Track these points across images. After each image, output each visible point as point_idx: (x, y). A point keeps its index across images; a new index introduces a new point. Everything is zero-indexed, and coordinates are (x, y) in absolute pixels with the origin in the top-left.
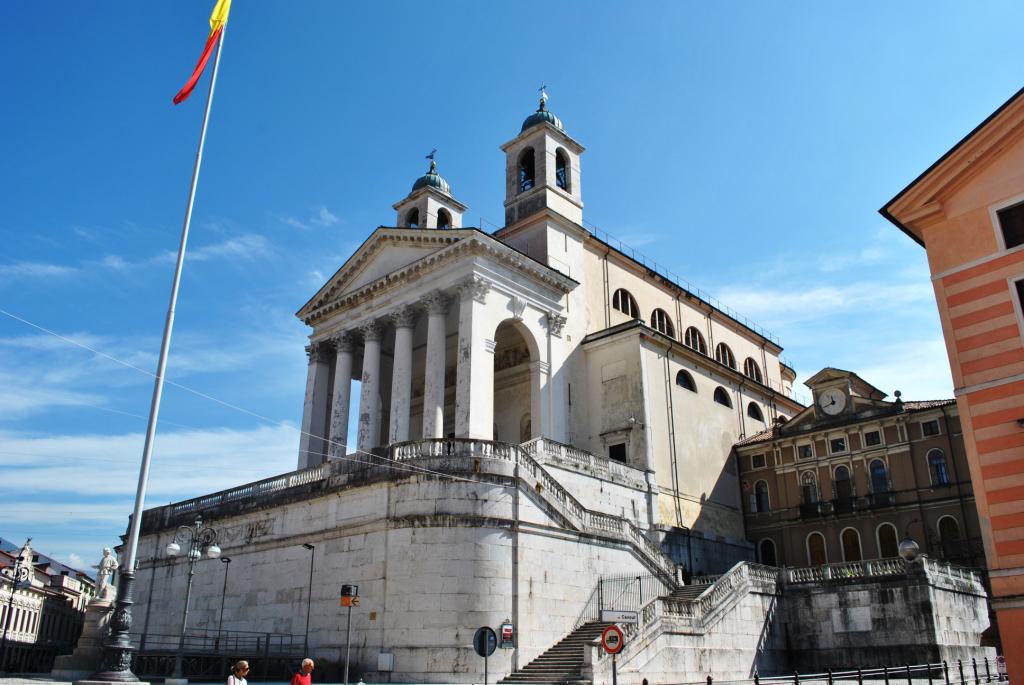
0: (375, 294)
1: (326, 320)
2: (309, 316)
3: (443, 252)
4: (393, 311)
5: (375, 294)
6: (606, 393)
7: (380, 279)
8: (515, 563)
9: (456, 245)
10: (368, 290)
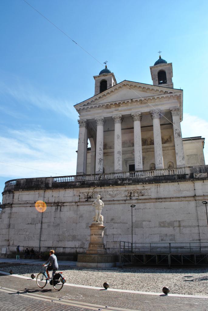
0: (121, 105)
1: (90, 111)
3: (160, 96)
4: (134, 113)
5: (121, 105)
6: (189, 159)
9: (171, 94)
10: (119, 103)
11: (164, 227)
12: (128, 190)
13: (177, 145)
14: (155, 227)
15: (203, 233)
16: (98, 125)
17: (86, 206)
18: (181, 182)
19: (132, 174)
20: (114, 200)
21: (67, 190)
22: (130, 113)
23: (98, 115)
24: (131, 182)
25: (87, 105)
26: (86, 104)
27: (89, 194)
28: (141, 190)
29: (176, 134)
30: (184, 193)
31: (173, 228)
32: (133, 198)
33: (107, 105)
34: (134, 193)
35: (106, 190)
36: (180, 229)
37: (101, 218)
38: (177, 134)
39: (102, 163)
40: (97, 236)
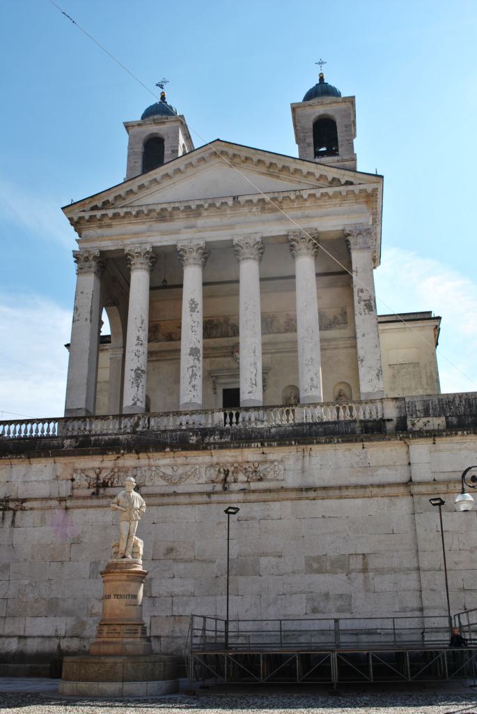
1: (110, 226)
3: (318, 193)
4: (242, 238)
5: (205, 213)
6: (394, 376)
9: (350, 188)
11: (319, 571)
12: (218, 464)
13: (364, 335)
14: (293, 572)
15: (432, 590)
17: (91, 511)
18: (370, 440)
19: (231, 415)
20: (175, 494)
21: (34, 460)
23: (134, 240)
24: (227, 439)
25: (101, 209)
26: (100, 205)
27: (103, 475)
28: (256, 465)
29: (359, 303)
30: (380, 472)
31: (347, 575)
32: (234, 487)
33: (163, 210)
34: (236, 471)
35: (152, 462)
36: (366, 579)
37: (135, 546)
38: (363, 303)
39: (143, 381)
40: (124, 601)
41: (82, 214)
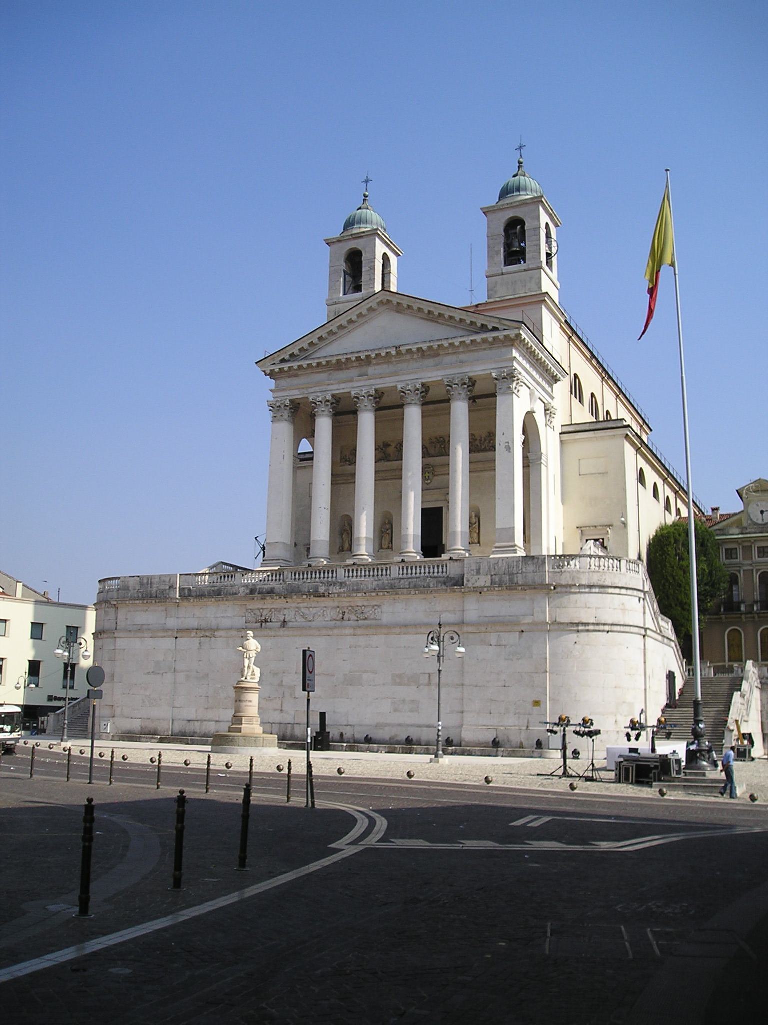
2: (277, 368)
5: (374, 362)
7: (390, 347)
8: (645, 662)
9: (495, 334)
10: (368, 357)
11: (400, 684)
14: (384, 684)
15: (470, 699)
16: (317, 414)
19: (349, 571)
22: (394, 384)
41: (273, 367)
